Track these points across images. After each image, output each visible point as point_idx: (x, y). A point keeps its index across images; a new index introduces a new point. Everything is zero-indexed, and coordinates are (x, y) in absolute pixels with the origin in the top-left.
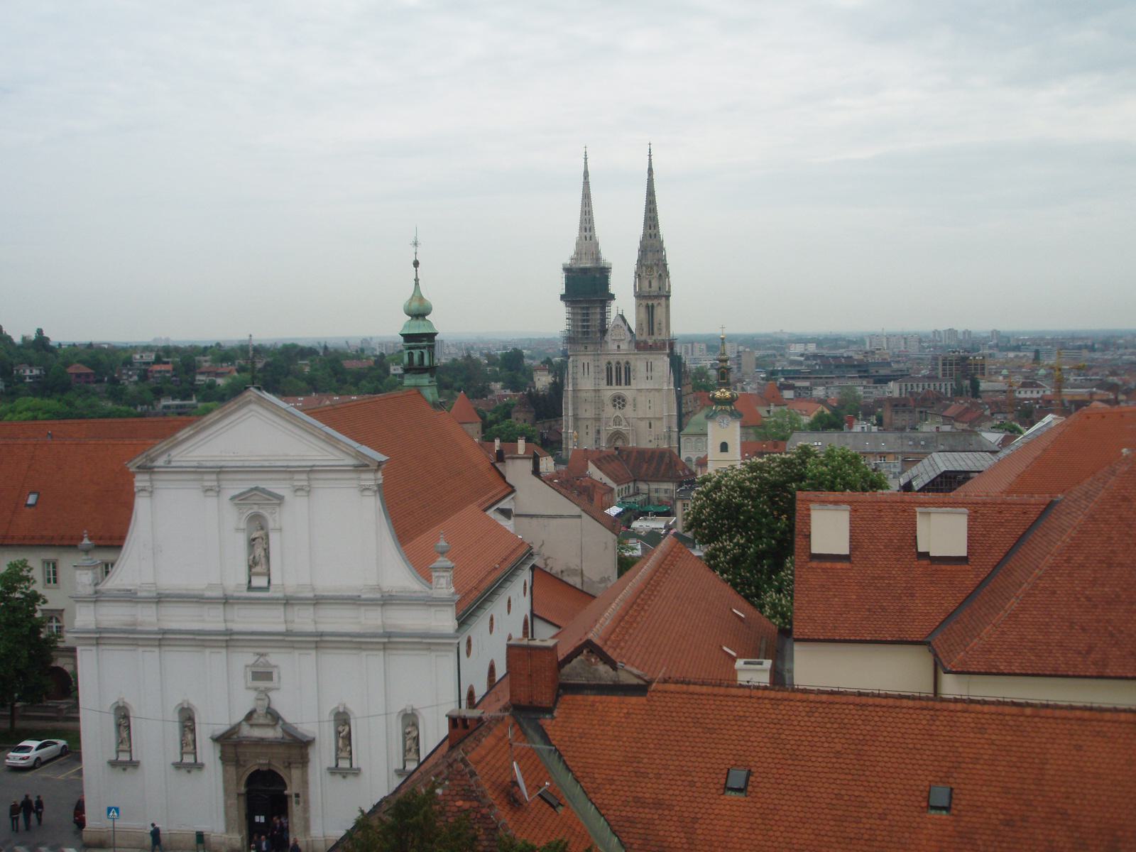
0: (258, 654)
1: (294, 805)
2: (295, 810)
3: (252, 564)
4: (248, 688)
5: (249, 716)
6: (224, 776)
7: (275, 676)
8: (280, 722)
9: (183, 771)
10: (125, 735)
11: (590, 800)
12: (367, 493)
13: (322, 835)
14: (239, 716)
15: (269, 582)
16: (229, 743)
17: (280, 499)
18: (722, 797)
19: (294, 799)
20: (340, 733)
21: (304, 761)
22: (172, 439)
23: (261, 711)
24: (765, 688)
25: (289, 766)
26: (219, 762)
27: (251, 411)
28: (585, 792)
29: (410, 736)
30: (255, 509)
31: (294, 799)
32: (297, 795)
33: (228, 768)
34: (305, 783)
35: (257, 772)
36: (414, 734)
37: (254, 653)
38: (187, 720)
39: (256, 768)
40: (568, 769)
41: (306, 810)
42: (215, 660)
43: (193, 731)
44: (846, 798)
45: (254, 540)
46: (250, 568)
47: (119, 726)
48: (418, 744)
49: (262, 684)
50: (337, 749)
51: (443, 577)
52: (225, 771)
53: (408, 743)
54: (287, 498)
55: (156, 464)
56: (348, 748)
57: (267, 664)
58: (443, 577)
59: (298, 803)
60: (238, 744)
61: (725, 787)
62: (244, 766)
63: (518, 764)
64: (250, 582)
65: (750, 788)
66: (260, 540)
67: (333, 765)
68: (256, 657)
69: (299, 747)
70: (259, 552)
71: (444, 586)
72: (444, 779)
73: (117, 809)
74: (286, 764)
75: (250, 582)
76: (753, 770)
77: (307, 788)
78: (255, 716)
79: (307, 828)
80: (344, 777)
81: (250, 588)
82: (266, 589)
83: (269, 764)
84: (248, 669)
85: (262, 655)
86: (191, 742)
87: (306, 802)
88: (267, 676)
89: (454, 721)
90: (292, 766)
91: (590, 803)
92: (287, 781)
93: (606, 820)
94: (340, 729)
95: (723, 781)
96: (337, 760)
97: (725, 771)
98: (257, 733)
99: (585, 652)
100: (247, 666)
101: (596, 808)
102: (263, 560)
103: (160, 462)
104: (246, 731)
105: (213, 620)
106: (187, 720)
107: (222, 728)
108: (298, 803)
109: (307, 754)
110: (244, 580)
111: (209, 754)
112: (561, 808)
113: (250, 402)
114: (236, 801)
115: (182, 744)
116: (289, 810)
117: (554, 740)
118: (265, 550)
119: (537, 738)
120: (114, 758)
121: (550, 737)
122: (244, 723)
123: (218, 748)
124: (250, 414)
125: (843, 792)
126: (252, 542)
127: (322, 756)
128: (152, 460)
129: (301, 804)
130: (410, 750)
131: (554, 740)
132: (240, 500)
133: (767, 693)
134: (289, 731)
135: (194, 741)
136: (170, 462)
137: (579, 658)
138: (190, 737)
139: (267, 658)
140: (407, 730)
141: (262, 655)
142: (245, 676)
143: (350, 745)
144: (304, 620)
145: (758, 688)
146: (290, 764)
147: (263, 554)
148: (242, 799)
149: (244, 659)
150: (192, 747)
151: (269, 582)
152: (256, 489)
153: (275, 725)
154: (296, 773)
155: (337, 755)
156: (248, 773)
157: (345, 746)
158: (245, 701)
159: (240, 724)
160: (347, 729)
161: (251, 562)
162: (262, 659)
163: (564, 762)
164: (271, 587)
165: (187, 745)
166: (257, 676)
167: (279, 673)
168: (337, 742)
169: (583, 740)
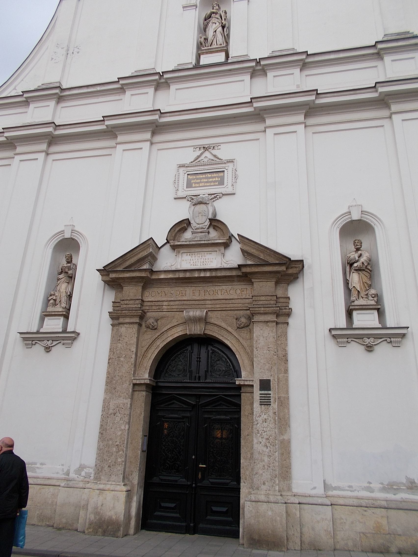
1: (256, 405)
6: (112, 350)
7: (228, 176)
9: (38, 349)
13: (320, 491)
19: (257, 392)
20: (351, 265)
26: (107, 321)
31: (257, 392)
33: (123, 329)
37: (195, 147)
39: (177, 332)
43: (71, 278)
45: (208, 18)
46: (200, 45)
50: (348, 290)
56: (372, 291)
57: (217, 160)
62: (154, 329)
66: (218, 16)
67: (342, 322)
74: (243, 320)
78: (188, 235)
80: (369, 348)
83: (205, 320)
84: (181, 169)
85: (205, 149)
86: (64, 299)
90: (256, 318)
96: (349, 313)
100: (181, 166)
102: (220, 39)
114: (129, 401)
118: (223, 27)
129: (274, 405)
135: (70, 297)
138: (63, 287)
139: (214, 152)
141: (205, 149)
142: (176, 182)
146: (250, 318)
147: (220, 29)
150: (64, 305)
153: (226, 245)
156: (161, 344)
162: (207, 154)
165: (55, 304)
168: (346, 283)
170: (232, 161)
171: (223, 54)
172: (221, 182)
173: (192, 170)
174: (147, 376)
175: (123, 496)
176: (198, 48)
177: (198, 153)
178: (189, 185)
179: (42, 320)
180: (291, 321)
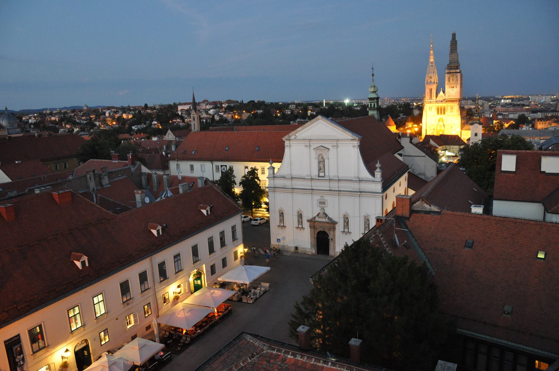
0: (321, 196)
1: (331, 242)
2: (331, 244)
3: (320, 169)
4: (318, 206)
5: (318, 215)
8: (328, 217)
9: (299, 230)
10: (282, 218)
11: (420, 247)
12: (355, 148)
14: (315, 215)
15: (325, 175)
16: (312, 221)
17: (329, 149)
18: (464, 249)
20: (345, 221)
21: (334, 229)
22: (296, 131)
23: (322, 213)
24: (481, 215)
25: (329, 230)
26: (309, 228)
27: (319, 122)
28: (418, 244)
29: (367, 223)
30: (321, 152)
31: (331, 240)
32: (332, 239)
33: (312, 230)
34: (334, 236)
35: (320, 231)
36: (368, 223)
38: (300, 216)
39: (320, 230)
40: (413, 237)
41: (334, 243)
42: (307, 198)
43: (302, 218)
44: (507, 252)
45: (320, 162)
46: (319, 170)
47: (280, 216)
48: (369, 226)
49: (322, 205)
51: (378, 175)
52: (311, 231)
53: (366, 225)
54: (330, 149)
55: (291, 138)
56: (348, 226)
58: (378, 175)
59: (332, 241)
60: (315, 221)
61: (465, 246)
63: (397, 235)
64: (319, 174)
65: (473, 247)
67: (343, 231)
68: (321, 197)
69: (333, 224)
70: (321, 165)
71: (379, 177)
72: (373, 238)
73: (280, 240)
75: (319, 174)
76: (475, 241)
77: (335, 237)
78: (320, 215)
79: (334, 249)
81: (319, 176)
82: (324, 177)
85: (322, 197)
87: (335, 241)
88: (324, 203)
89: (378, 220)
91: (419, 248)
92: (329, 234)
93: (424, 253)
94: (345, 220)
95: (464, 244)
97: (466, 241)
98: (320, 220)
99: (421, 200)
100: (318, 200)
101: (421, 250)
102: (323, 168)
103: (293, 137)
104: (317, 219)
105: (307, 185)
106: (300, 216)
107: (310, 217)
108: (332, 241)
109: (335, 227)
110: (317, 174)
111: (306, 225)
112: (410, 249)
113: (319, 119)
115: (298, 222)
116: (329, 243)
117: (409, 227)
119: (404, 226)
120: (279, 225)
121: (408, 227)
122: (316, 217)
123: (309, 223)
124: (319, 123)
125: (506, 251)
126: (319, 162)
127: (340, 227)
128: (290, 137)
130: (367, 227)
131: (409, 227)
132: (316, 149)
133: (481, 216)
134: (329, 218)
135: (302, 221)
136: (296, 138)
137: (419, 202)
140: (366, 222)
143: (348, 225)
144: (334, 185)
145: (479, 214)
147: (323, 166)
148: (316, 239)
149: (317, 197)
151: (325, 175)
152: (321, 146)
154: (332, 232)
155: (344, 228)
156: (317, 232)
157: (347, 225)
158: (317, 210)
159: (315, 217)
160: (347, 220)
161: (319, 169)
162: (322, 198)
163: (412, 235)
164: (325, 177)
166: (321, 203)
167: (327, 202)
169: (419, 228)
170: (327, 200)
171: (324, 174)
172: (325, 204)
173: (320, 201)
174: (316, 236)
175: (315, 251)
176: (319, 171)
177: (321, 197)
178: (320, 204)
179: (298, 225)
180: (336, 230)
